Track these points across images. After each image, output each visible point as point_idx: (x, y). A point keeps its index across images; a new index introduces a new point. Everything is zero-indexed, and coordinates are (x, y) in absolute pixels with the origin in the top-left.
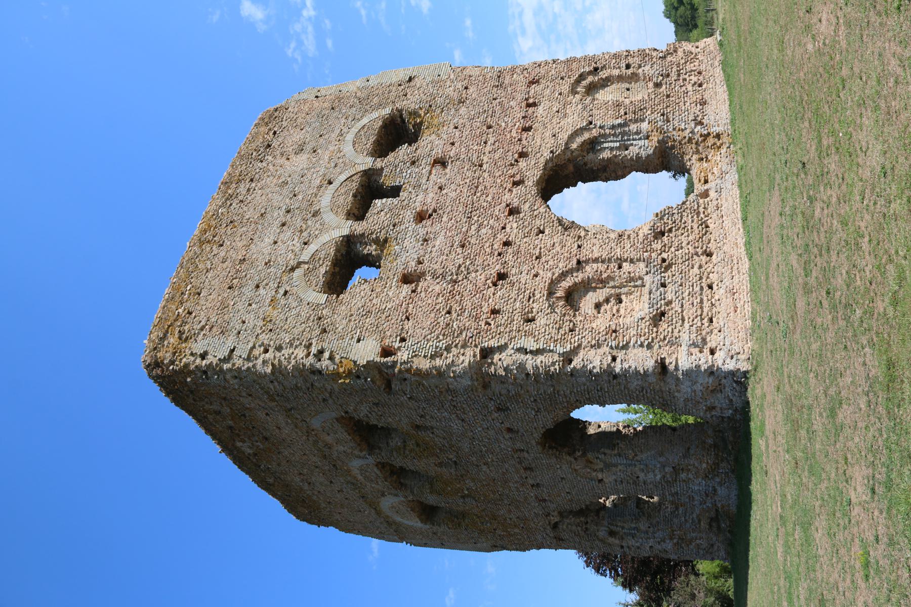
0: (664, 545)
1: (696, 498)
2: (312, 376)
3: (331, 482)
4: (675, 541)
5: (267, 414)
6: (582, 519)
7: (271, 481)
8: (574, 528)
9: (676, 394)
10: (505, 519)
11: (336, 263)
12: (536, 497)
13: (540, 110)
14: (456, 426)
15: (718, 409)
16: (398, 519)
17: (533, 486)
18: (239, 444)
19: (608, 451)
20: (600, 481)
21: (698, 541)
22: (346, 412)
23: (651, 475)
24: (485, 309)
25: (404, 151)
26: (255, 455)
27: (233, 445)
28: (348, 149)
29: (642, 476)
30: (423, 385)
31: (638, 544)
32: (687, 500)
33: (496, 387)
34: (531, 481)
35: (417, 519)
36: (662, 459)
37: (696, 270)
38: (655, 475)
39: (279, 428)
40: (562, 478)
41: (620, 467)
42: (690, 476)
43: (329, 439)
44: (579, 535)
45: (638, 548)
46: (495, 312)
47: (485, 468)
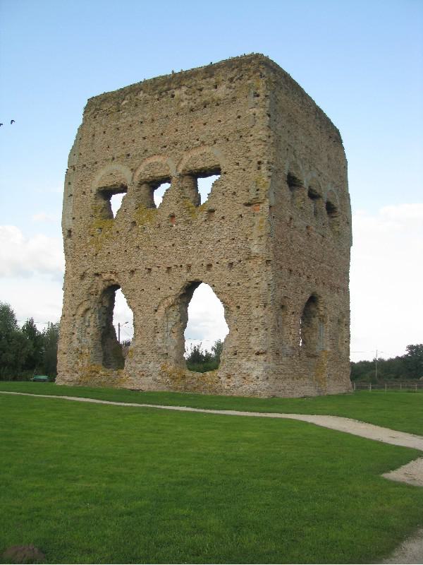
0: (76, 342)
1: (139, 366)
2: (256, 162)
3: (144, 138)
5: (220, 121)
6: (100, 293)
7: (141, 94)
8: (95, 287)
11: (294, 178)
12: (136, 270)
13: (336, 295)
14: (215, 236)
16: (102, 172)
18: (184, 89)
19: (178, 318)
21: (80, 365)
22: (225, 173)
24: (283, 263)
25: (327, 219)
26: (173, 96)
28: (329, 187)
29: (160, 335)
32: (137, 360)
34: (154, 269)
35: (101, 186)
36: (172, 347)
37: (291, 372)
38: (161, 343)
39: (205, 124)
43: (196, 153)
44: (89, 289)
46: (281, 268)
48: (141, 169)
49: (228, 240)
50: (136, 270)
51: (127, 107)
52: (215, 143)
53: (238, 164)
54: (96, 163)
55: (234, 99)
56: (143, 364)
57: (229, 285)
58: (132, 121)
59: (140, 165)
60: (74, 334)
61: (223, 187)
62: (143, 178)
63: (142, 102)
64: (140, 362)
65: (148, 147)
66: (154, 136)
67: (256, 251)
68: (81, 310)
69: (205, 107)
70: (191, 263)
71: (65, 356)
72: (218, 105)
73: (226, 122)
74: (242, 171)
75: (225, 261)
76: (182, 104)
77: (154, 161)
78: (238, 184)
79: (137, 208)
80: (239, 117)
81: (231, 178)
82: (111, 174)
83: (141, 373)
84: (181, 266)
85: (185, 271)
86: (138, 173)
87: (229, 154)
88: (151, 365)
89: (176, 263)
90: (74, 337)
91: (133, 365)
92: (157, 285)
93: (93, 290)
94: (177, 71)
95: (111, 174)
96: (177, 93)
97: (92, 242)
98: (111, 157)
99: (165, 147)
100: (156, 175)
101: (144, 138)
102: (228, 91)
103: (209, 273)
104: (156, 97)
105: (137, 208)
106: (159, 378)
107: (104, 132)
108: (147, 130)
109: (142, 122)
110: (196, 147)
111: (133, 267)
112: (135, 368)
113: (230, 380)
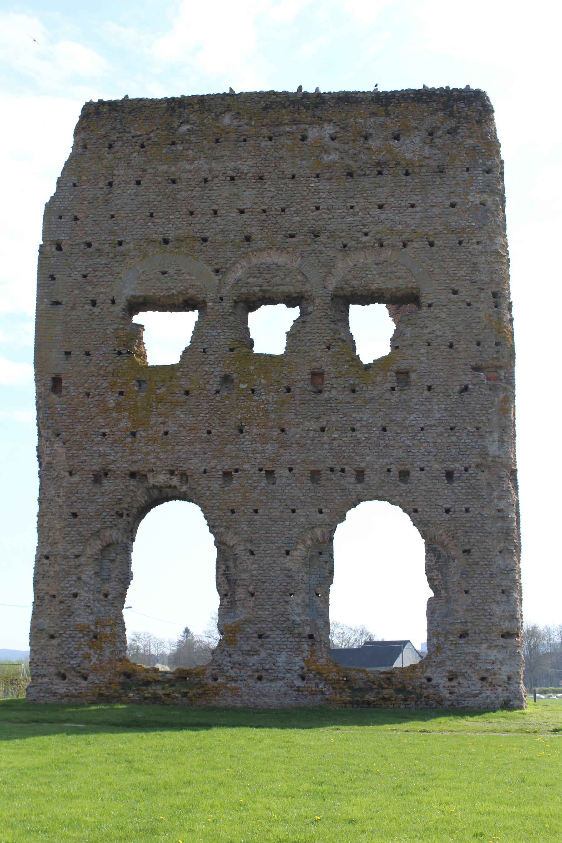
1: (252, 660)
3: (242, 212)
4: (93, 628)
5: (413, 206)
7: (227, 119)
8: (129, 499)
9: (484, 646)
10: (160, 415)
12: (236, 471)
15: (448, 684)
17: (270, 473)
18: (329, 129)
20: (288, 553)
22: (430, 305)
23: (298, 610)
26: (304, 138)
27: (330, 121)
30: (491, 408)
31: (84, 577)
32: (246, 648)
33: (484, 477)
34: (281, 472)
35: (138, 293)
38: (299, 615)
39: (381, 207)
40: (293, 511)
41: (306, 577)
42: (306, 654)
45: (79, 578)
47: (314, 425)
48: (239, 272)
49: (440, 429)
50: (236, 471)
51: (193, 138)
52: (405, 246)
53: (455, 292)
54: (120, 243)
55: (441, 170)
56: (263, 654)
57: (447, 511)
58: (210, 170)
59: (234, 264)
60: (75, 595)
61: (428, 331)
62: (244, 290)
63: (233, 136)
64: (254, 652)
65: (253, 230)
66: (264, 211)
67: (497, 453)
68: (97, 545)
69: (380, 173)
70: (363, 465)
71: (55, 642)
72: (407, 174)
73: (426, 210)
74: (464, 305)
75: (437, 466)
76: (327, 158)
77: (269, 260)
78: (457, 329)
79: (232, 350)
80: (453, 205)
81: (443, 315)
82: (164, 273)
83: (256, 675)
84: (343, 470)
85: (353, 480)
86: (231, 279)
87: (437, 271)
88: (282, 659)
89: (330, 462)
90: (77, 604)
92: (288, 503)
93: (126, 506)
94: (310, 89)
95: (164, 273)
96: (313, 133)
97: (118, 407)
98: (160, 238)
99: (292, 236)
100: (275, 289)
101: (242, 212)
102: (427, 151)
103: (404, 486)
104: (265, 131)
105: (232, 350)
106: (298, 683)
107: (138, 183)
108: (249, 196)
109: (232, 178)
110: (365, 248)
111: (227, 465)
112: (243, 665)
113: (454, 683)
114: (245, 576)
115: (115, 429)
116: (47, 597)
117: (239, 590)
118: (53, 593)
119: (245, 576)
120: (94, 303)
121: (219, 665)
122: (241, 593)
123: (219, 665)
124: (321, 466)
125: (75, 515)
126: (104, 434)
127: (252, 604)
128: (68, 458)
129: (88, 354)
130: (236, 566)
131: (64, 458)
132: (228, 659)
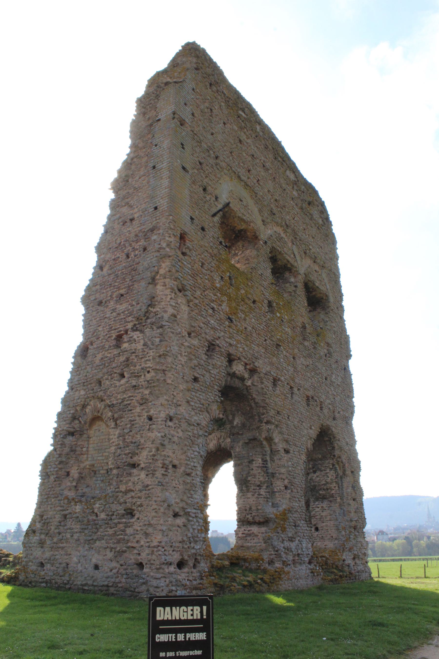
1: (293, 545)
32: (290, 535)
34: (295, 390)
70: (322, 400)
91: (287, 544)
95: (241, 201)
114: (283, 470)
115: (220, 308)
116: (170, 467)
117: (278, 482)
118: (176, 462)
119: (283, 470)
120: (205, 190)
121: (277, 551)
122: (278, 485)
123: (277, 551)
124: (310, 393)
125: (196, 379)
126: (213, 309)
127: (288, 496)
128: (191, 318)
129: (203, 229)
130: (272, 460)
131: (186, 316)
132: (282, 545)
